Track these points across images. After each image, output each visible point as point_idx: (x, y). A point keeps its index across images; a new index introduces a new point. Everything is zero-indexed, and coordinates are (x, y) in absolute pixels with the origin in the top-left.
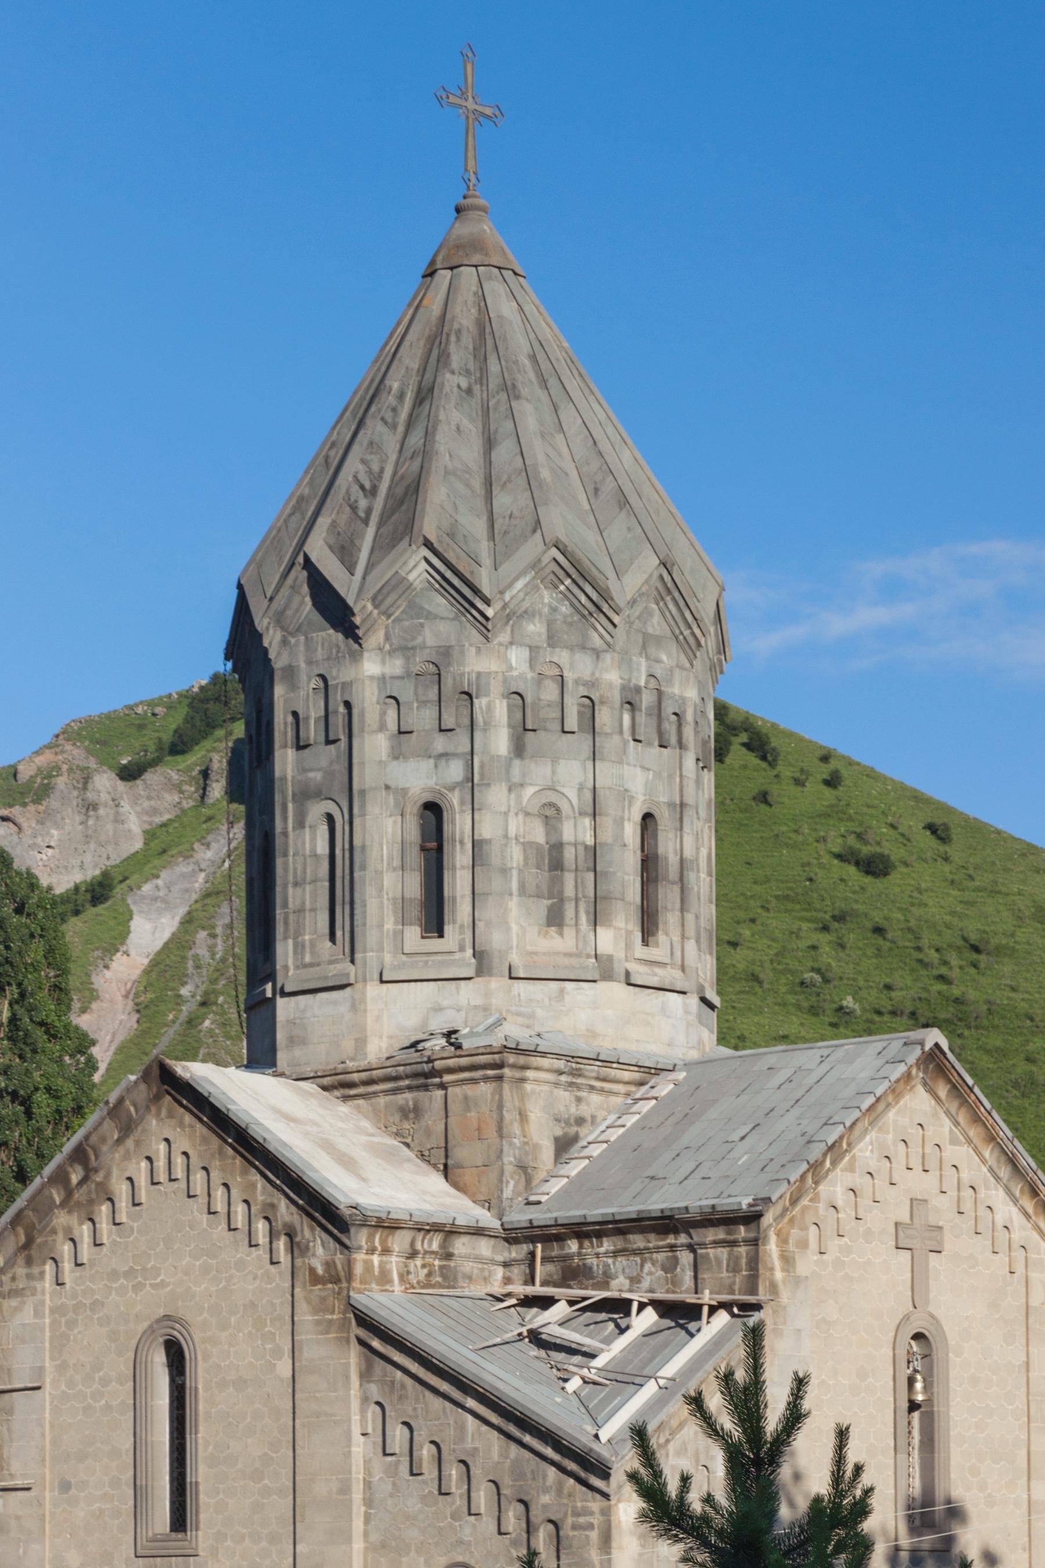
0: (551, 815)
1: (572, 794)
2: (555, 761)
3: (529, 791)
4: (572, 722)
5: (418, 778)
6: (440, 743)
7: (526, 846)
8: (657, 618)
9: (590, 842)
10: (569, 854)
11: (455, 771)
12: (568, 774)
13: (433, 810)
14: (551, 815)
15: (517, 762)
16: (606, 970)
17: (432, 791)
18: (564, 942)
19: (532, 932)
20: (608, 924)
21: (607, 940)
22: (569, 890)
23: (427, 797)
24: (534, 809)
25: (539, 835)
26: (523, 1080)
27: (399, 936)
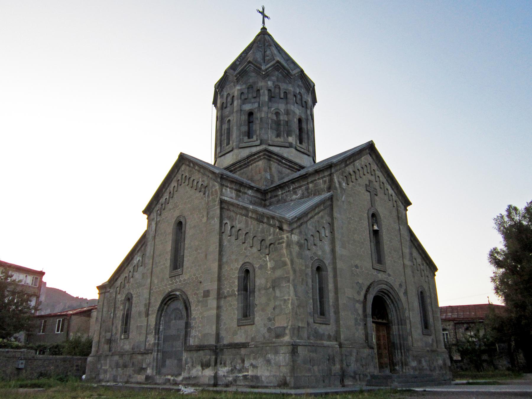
0: (277, 114)
1: (282, 110)
2: (278, 103)
4: (282, 96)
5: (247, 107)
6: (253, 100)
7: (272, 119)
9: (286, 120)
10: (282, 122)
11: (256, 105)
12: (282, 107)
13: (251, 114)
14: (277, 114)
15: (270, 103)
16: (290, 146)
18: (281, 140)
19: (274, 137)
20: (291, 136)
21: (290, 139)
22: (282, 129)
25: (275, 118)
26: (270, 160)
27: (243, 139)
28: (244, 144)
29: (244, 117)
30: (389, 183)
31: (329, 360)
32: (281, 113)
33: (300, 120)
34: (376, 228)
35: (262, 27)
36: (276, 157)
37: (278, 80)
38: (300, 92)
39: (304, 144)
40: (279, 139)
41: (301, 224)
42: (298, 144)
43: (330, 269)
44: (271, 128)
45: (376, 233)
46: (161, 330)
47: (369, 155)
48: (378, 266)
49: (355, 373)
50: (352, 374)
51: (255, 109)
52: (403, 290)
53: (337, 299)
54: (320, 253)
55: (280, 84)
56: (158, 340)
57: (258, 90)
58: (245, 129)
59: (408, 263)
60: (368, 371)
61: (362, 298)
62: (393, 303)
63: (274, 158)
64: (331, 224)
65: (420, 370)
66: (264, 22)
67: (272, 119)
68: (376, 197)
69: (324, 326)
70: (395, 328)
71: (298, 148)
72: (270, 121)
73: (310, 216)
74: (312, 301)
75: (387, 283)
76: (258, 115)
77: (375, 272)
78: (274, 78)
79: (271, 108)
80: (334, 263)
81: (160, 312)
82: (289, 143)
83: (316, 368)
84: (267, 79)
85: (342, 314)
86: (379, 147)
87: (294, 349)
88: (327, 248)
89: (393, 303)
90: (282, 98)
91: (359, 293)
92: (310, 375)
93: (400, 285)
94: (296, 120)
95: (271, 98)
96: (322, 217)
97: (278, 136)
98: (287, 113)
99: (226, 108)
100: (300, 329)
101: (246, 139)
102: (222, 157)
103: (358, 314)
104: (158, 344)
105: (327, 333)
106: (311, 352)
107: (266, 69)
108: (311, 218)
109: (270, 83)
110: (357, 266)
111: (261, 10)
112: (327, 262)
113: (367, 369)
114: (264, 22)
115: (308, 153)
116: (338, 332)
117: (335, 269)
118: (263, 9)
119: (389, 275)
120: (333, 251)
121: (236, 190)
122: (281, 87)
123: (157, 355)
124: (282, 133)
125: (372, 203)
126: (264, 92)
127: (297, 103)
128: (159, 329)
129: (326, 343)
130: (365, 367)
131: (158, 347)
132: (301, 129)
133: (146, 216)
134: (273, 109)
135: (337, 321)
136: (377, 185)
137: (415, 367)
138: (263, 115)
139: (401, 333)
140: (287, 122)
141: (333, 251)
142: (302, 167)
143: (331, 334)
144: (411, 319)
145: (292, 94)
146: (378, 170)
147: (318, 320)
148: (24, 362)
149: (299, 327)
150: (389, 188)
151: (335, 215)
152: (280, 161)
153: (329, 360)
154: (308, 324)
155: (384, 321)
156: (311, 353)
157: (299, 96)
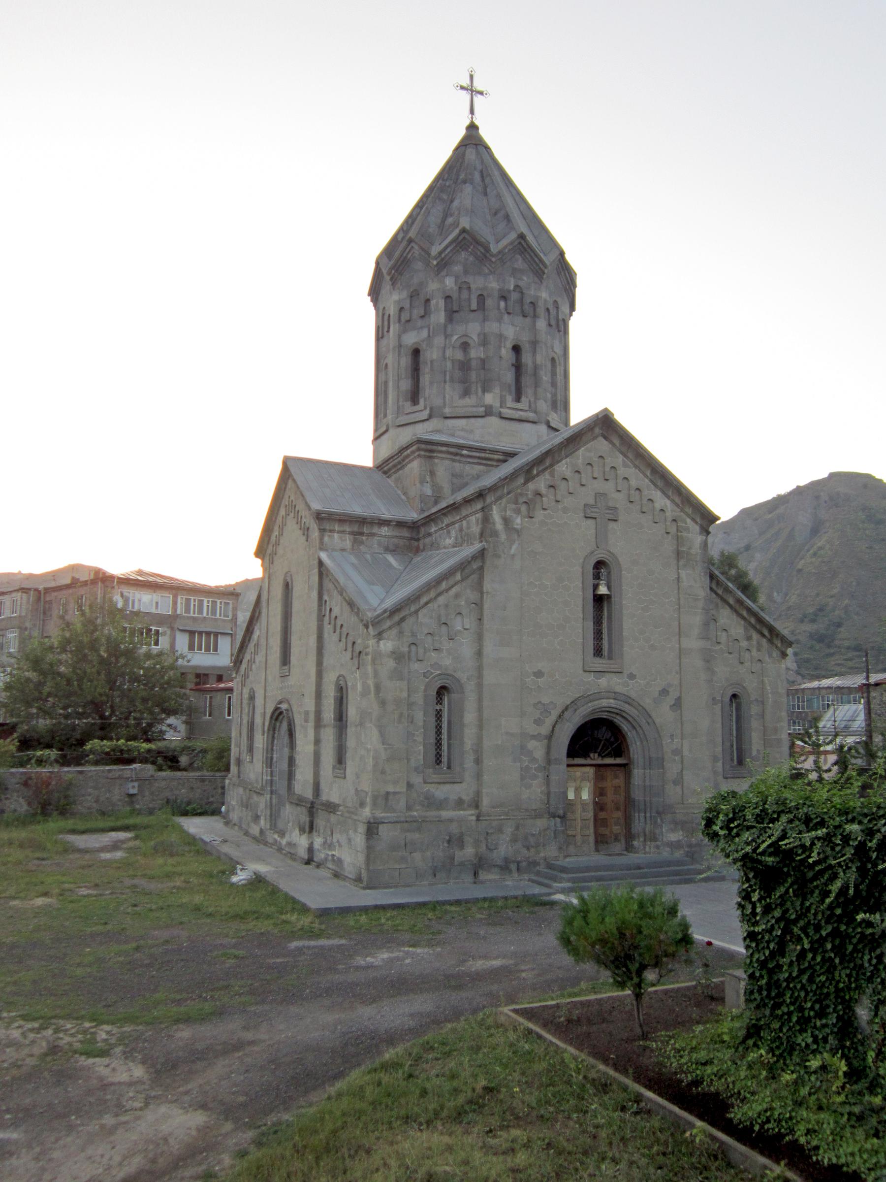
0: (465, 346)
1: (475, 338)
3: (455, 337)
4: (474, 306)
5: (411, 339)
6: (420, 323)
8: (520, 261)
9: (482, 356)
10: (474, 364)
12: (473, 329)
13: (416, 352)
16: (489, 412)
17: (416, 343)
20: (489, 391)
23: (415, 346)
24: (458, 344)
25: (459, 355)
28: (406, 417)
29: (406, 361)
30: (655, 485)
31: (449, 842)
32: (470, 341)
33: (516, 349)
34: (603, 590)
35: (468, 122)
36: (444, 449)
37: (466, 272)
38: (517, 286)
39: (523, 398)
40: (468, 401)
41: (403, 620)
42: (510, 402)
43: (470, 689)
44: (452, 380)
45: (599, 600)
46: (275, 759)
47: (601, 439)
48: (599, 664)
49: (507, 860)
50: (499, 862)
51: (423, 341)
52: (670, 700)
53: (480, 738)
54: (447, 662)
55: (470, 279)
56: (272, 775)
57: (428, 301)
58: (406, 385)
59: (693, 643)
60: (542, 855)
61: (545, 730)
62: (634, 728)
63: (441, 452)
64: (479, 605)
65: (690, 846)
66: (472, 112)
67: (453, 361)
68: (612, 525)
69: (447, 787)
70: (637, 773)
71: (506, 412)
72: (449, 364)
73: (424, 600)
74: (421, 748)
75: (616, 696)
76: (431, 354)
77: (591, 677)
78: (457, 268)
79: (452, 335)
80: (480, 676)
81: (271, 732)
82: (486, 406)
83: (417, 856)
84: (444, 273)
85: (489, 762)
86: (623, 418)
87: (372, 829)
88: (467, 650)
89: (634, 728)
90: (474, 311)
91: (538, 722)
92: (404, 866)
93: (664, 692)
94: (506, 353)
95: (452, 314)
96: (457, 596)
97: (466, 393)
98: (484, 341)
99: (382, 337)
100: (391, 797)
101: (408, 406)
102: (400, 429)
103: (534, 760)
104: (272, 781)
105: (453, 797)
106: (408, 831)
107: (440, 253)
108: (427, 603)
109: (449, 282)
110: (539, 674)
111: (466, 82)
112: (463, 676)
113: (538, 852)
114: (472, 112)
115: (531, 415)
116: (478, 794)
117: (480, 686)
118: (471, 77)
119: (632, 676)
120: (479, 654)
121: (352, 533)
122: (473, 286)
123: (271, 798)
124: (473, 389)
125: (601, 537)
126: (437, 303)
127: (509, 313)
128: (272, 758)
129: (445, 814)
130: (532, 850)
131: (271, 786)
132: (518, 367)
133: (259, 561)
134: (455, 337)
135: (479, 776)
136: (619, 500)
137: (679, 841)
138: (435, 357)
139: (647, 783)
140: (483, 361)
141: (479, 654)
142: (512, 455)
143: (464, 797)
144: (686, 753)
145: (496, 294)
146: (625, 465)
147: (435, 778)
148: (136, 784)
149: (388, 793)
150: (657, 495)
151: (487, 586)
152: (456, 454)
153: (449, 842)
154: (409, 786)
155: (619, 761)
156: (408, 834)
157: (515, 296)
